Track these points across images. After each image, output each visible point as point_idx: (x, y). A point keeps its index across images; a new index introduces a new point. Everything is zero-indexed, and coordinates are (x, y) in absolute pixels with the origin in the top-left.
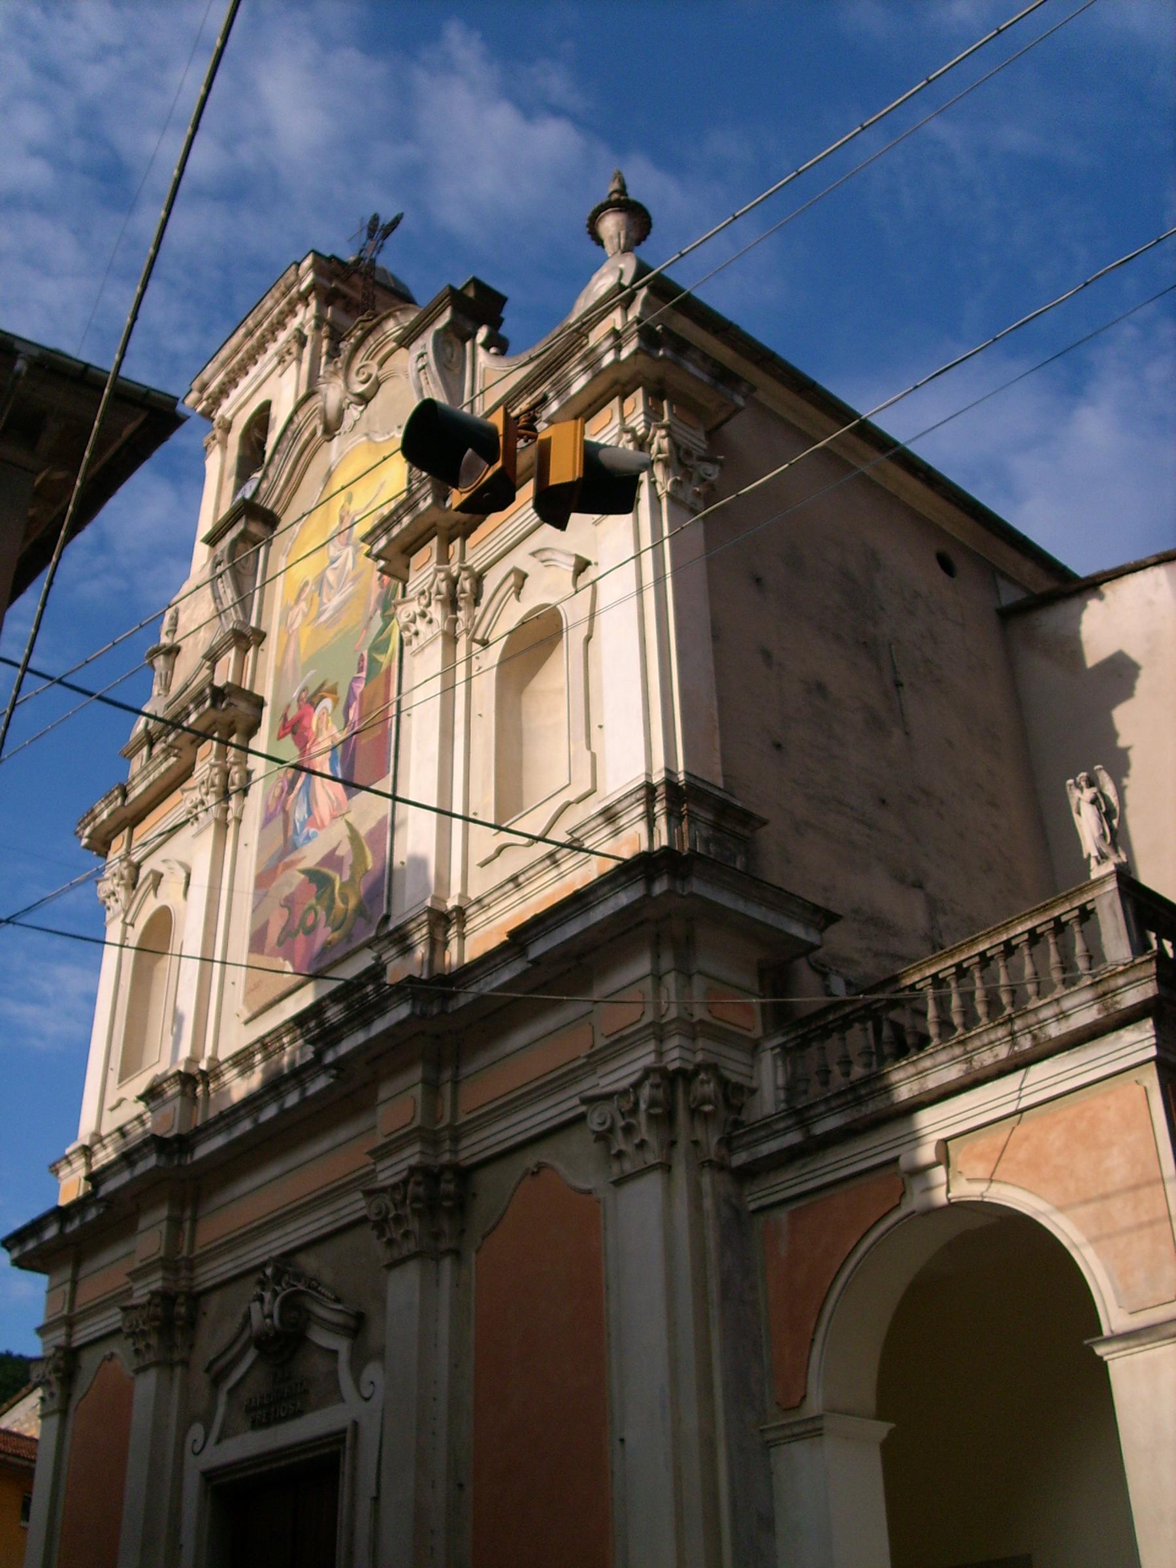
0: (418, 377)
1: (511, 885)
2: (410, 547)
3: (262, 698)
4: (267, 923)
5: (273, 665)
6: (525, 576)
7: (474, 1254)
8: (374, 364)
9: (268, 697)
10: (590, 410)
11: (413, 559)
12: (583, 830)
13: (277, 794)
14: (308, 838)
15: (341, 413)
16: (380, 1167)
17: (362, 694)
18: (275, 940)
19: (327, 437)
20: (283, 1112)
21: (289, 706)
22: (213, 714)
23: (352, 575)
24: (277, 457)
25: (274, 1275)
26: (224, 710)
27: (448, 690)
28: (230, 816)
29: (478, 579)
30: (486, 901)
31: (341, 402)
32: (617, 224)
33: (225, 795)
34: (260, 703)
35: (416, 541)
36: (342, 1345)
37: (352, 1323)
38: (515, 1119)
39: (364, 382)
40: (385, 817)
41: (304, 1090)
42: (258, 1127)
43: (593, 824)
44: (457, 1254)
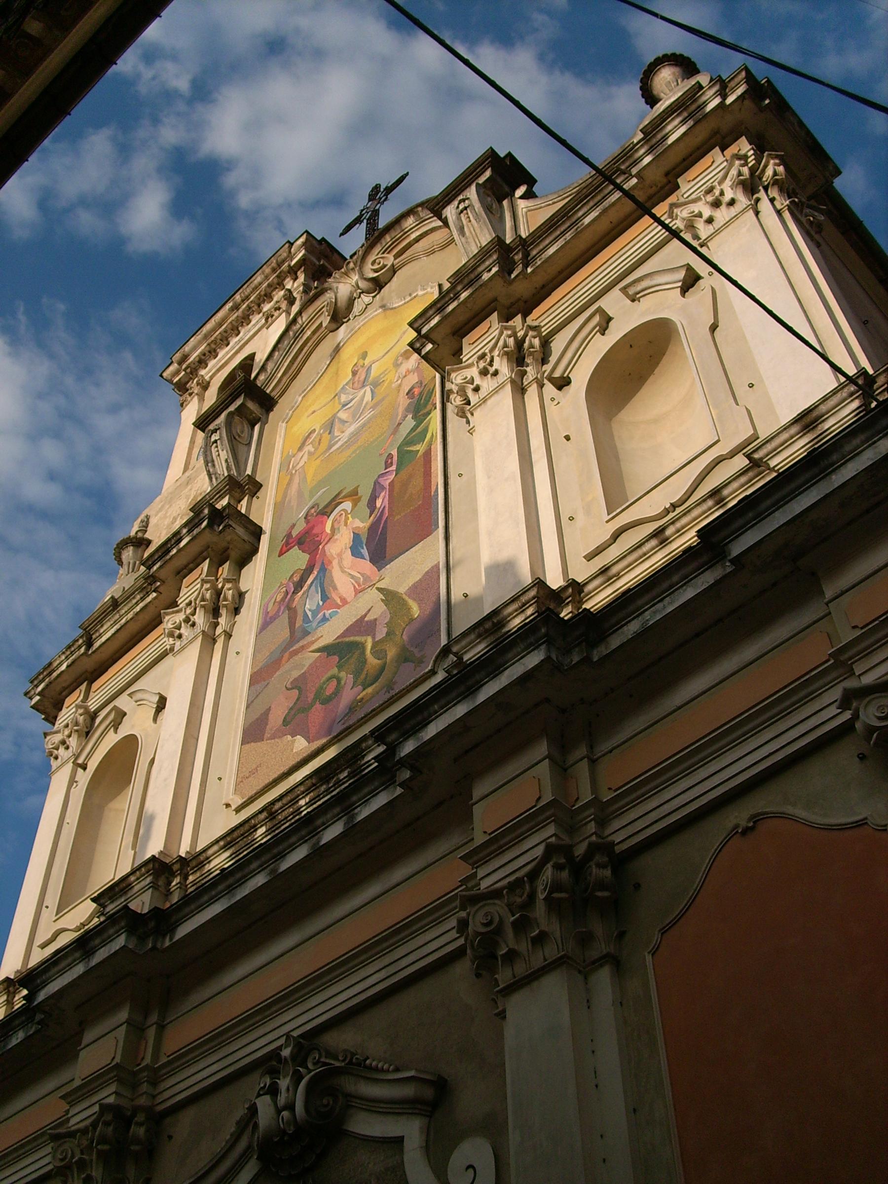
0: (459, 219)
1: (653, 542)
2: (463, 328)
3: (261, 528)
4: (269, 709)
5: (272, 502)
6: (610, 319)
7: (649, 958)
8: (391, 257)
9: (266, 525)
10: (685, 163)
11: (465, 341)
12: (769, 447)
13: (279, 598)
14: (325, 619)
15: (351, 302)
16: (481, 873)
17: (391, 484)
18: (280, 721)
19: (334, 326)
20: (318, 852)
21: (294, 526)
22: (208, 537)
23: (371, 404)
24: (277, 353)
25: (293, 1056)
26: (221, 532)
27: (733, 78)
28: (219, 630)
29: (546, 343)
30: (614, 570)
31: (352, 293)
32: (674, 74)
33: (215, 612)
34: (257, 532)
35: (469, 321)
36: (411, 1130)
37: (428, 1093)
38: (703, 773)
39: (376, 271)
40: (435, 569)
41: (353, 817)
42: (277, 878)
43: (785, 436)
44: (616, 962)
